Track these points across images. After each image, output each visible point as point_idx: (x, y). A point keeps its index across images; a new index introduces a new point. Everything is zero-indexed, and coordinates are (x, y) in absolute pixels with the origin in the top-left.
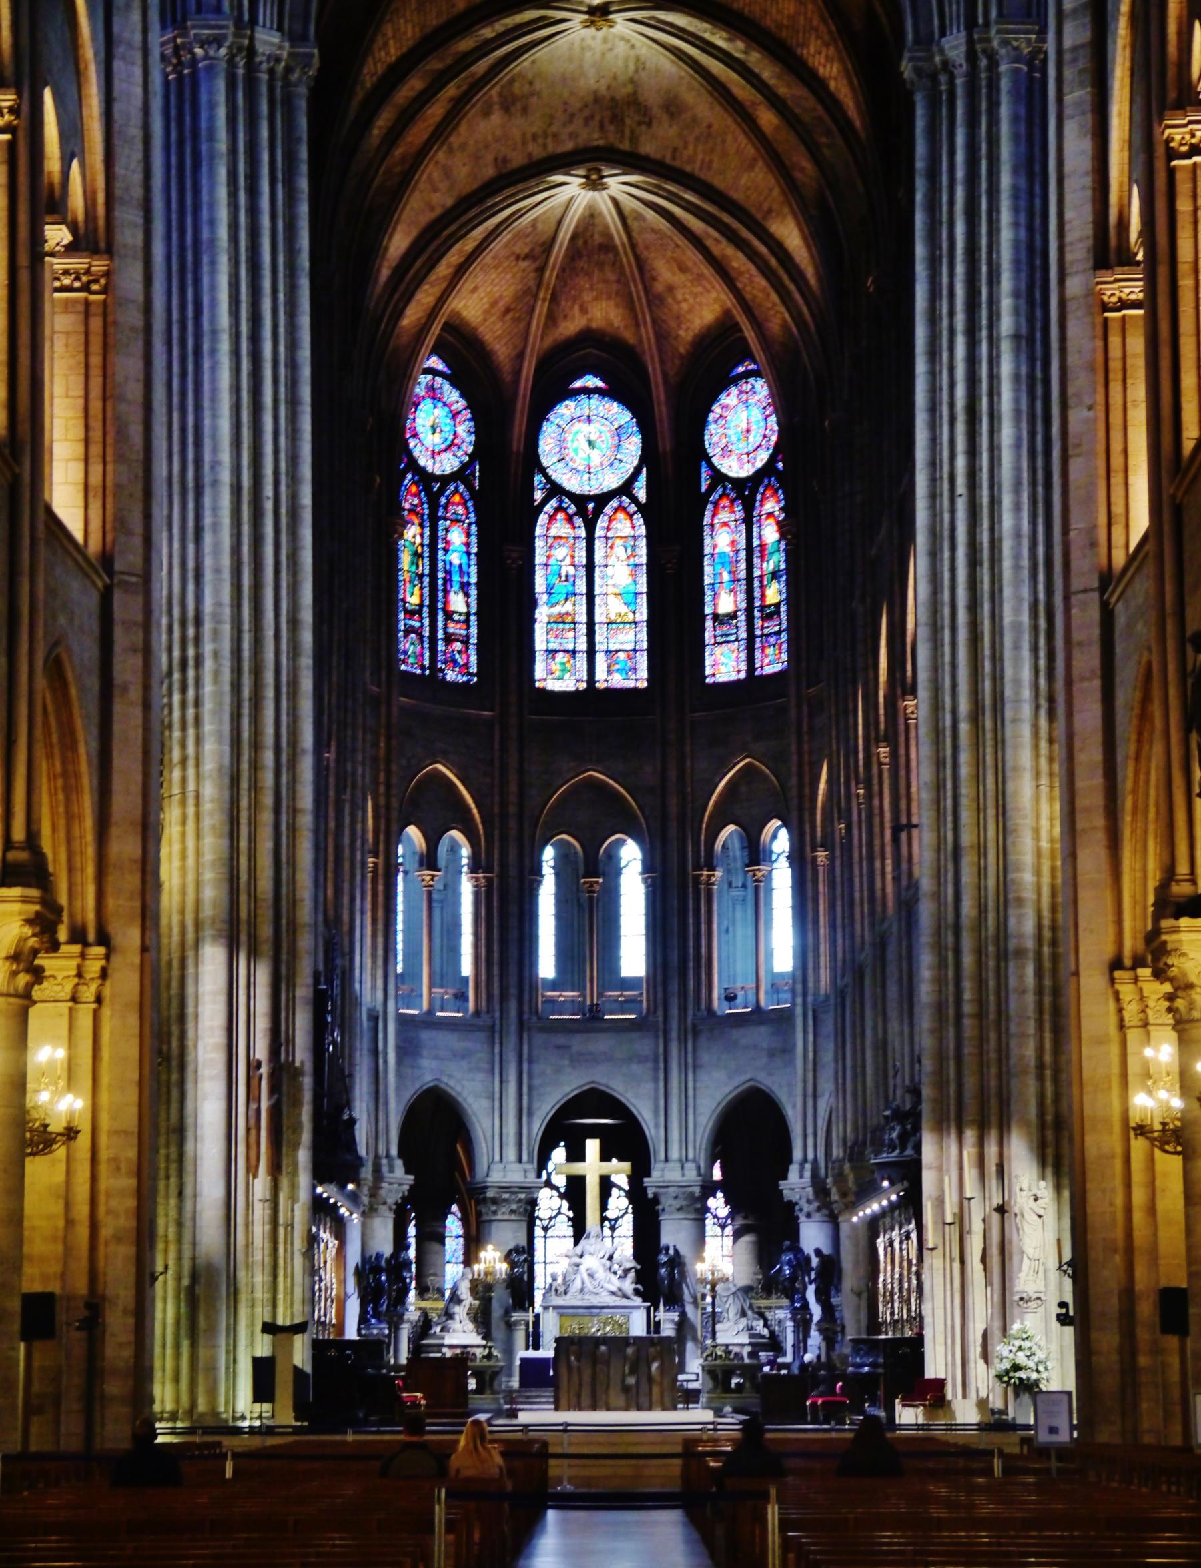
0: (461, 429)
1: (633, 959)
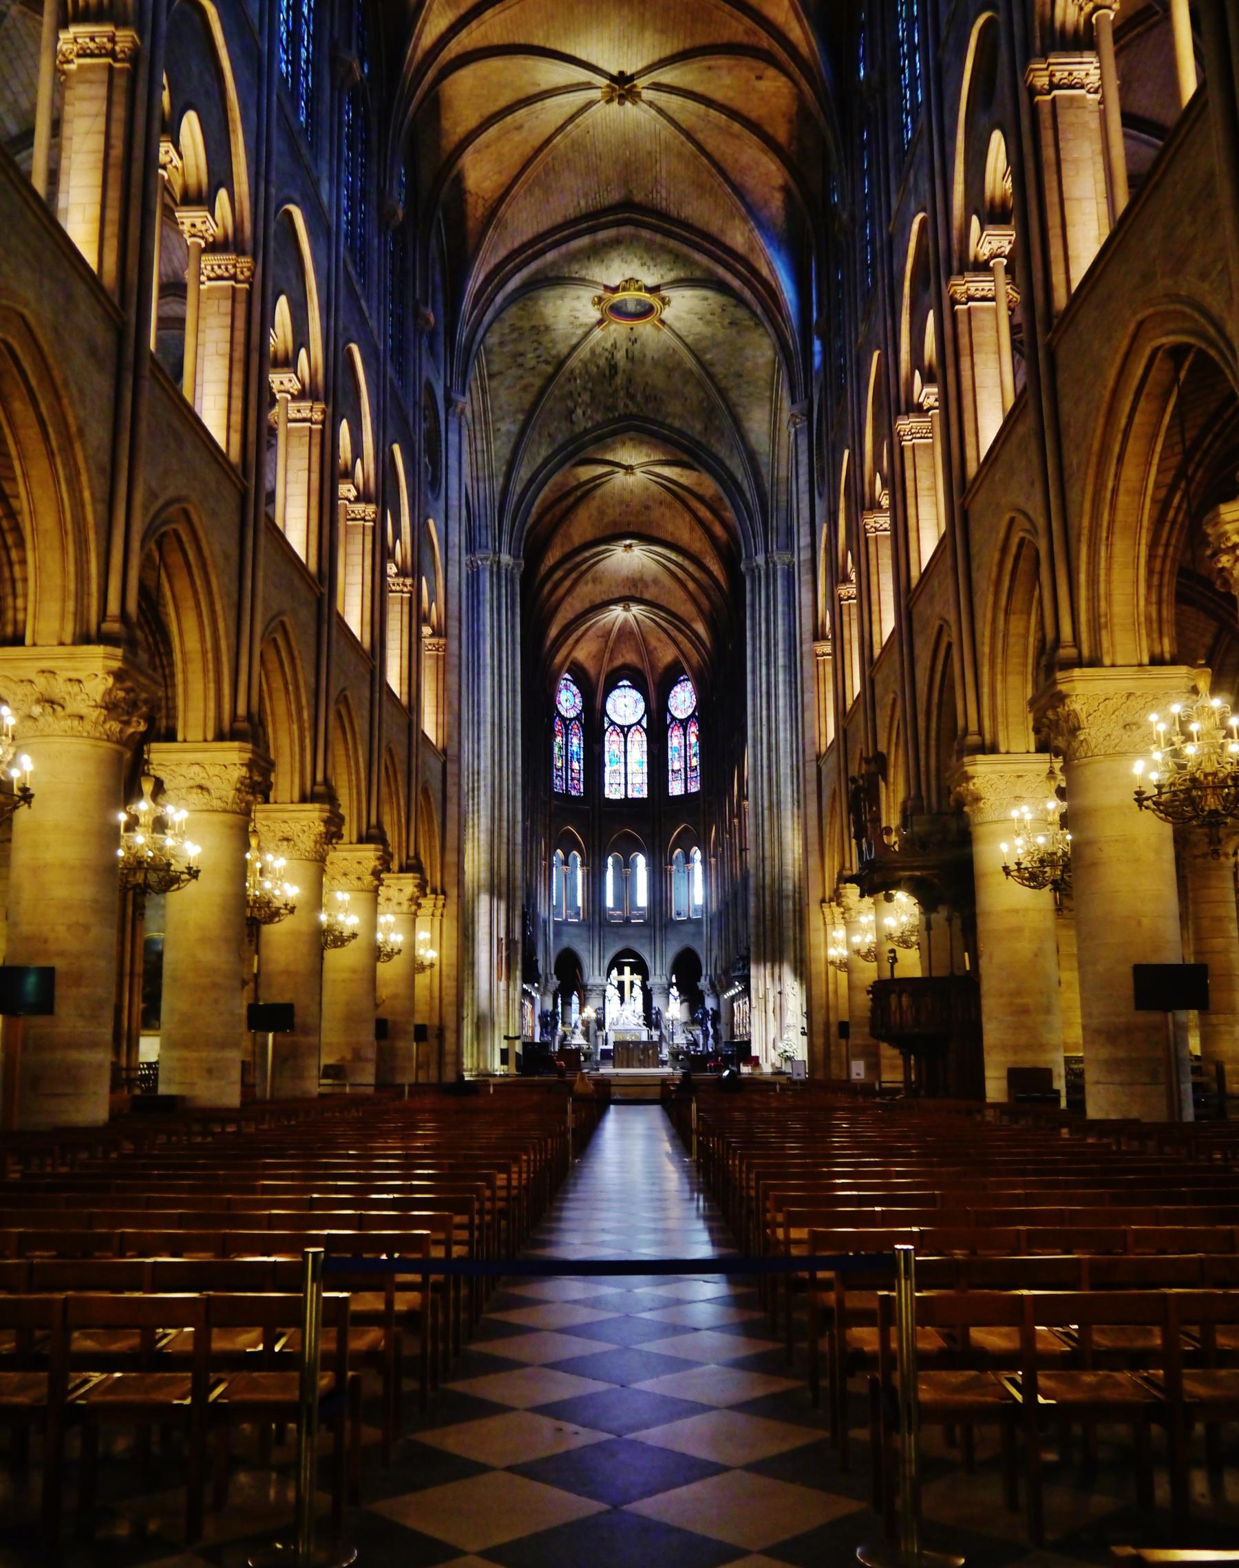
0: (578, 700)
1: (642, 899)
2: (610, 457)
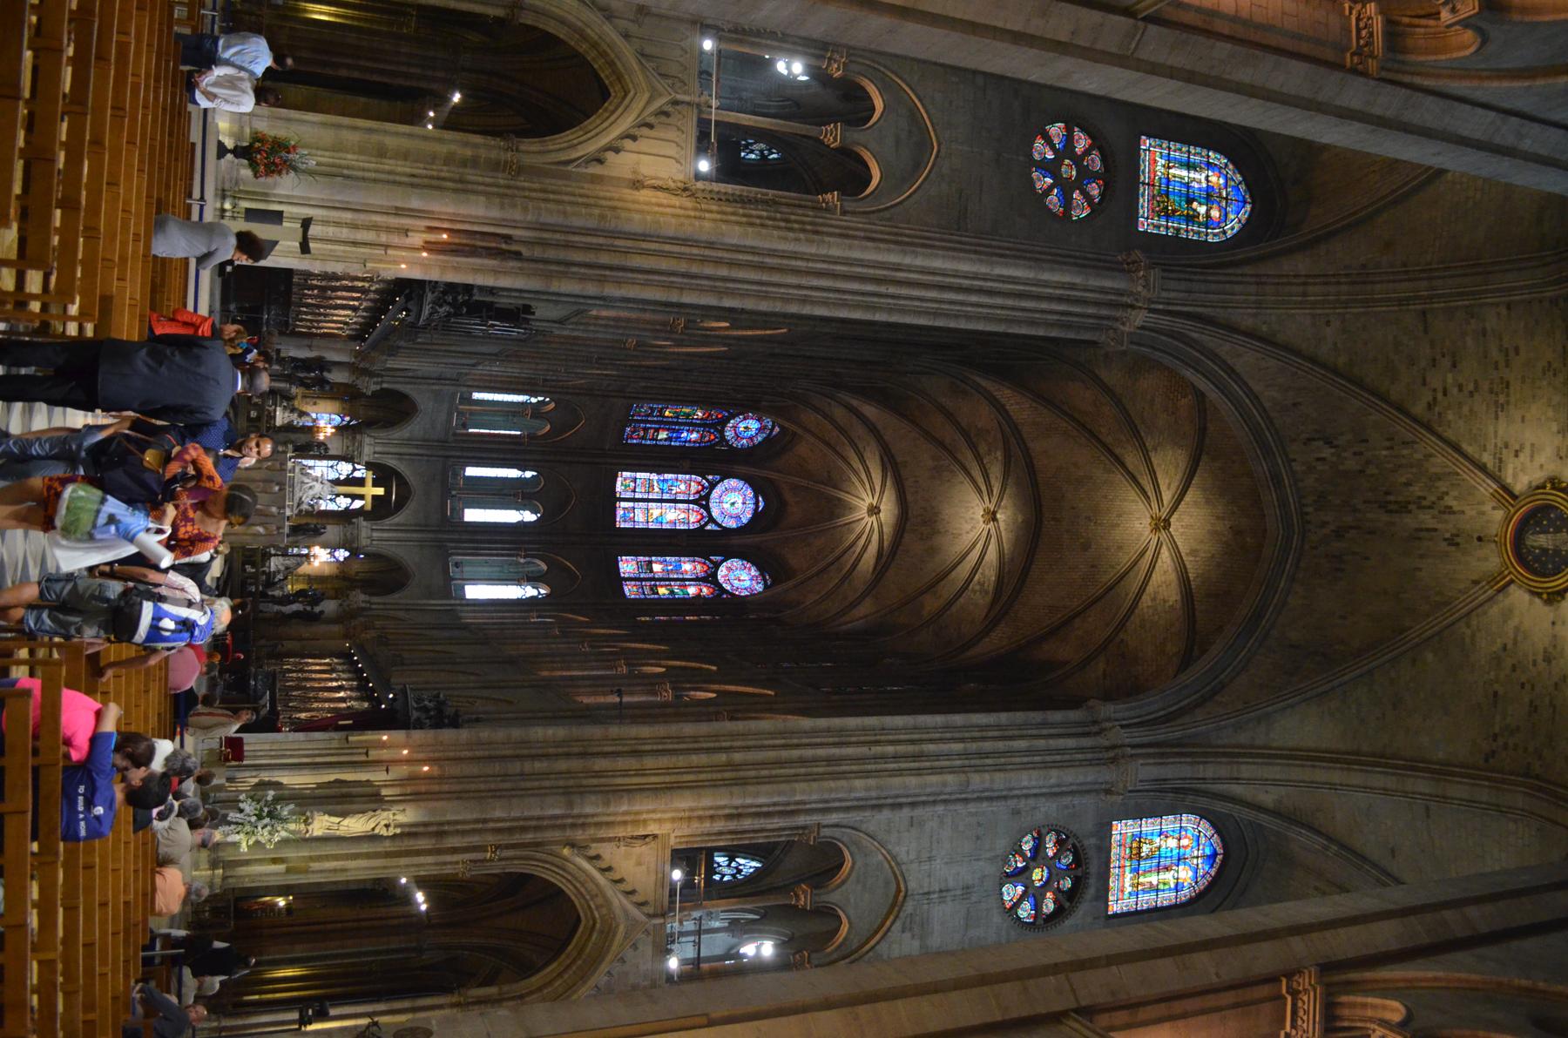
1: (472, 515)
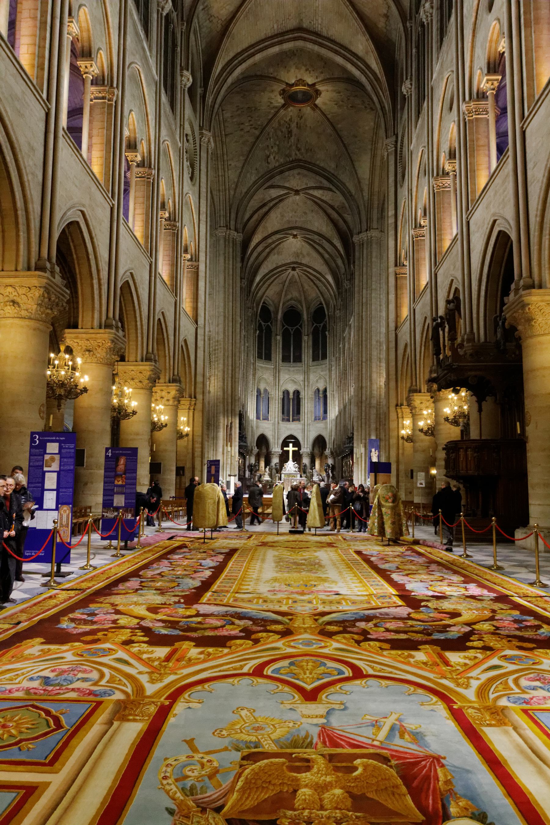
2: (287, 185)
